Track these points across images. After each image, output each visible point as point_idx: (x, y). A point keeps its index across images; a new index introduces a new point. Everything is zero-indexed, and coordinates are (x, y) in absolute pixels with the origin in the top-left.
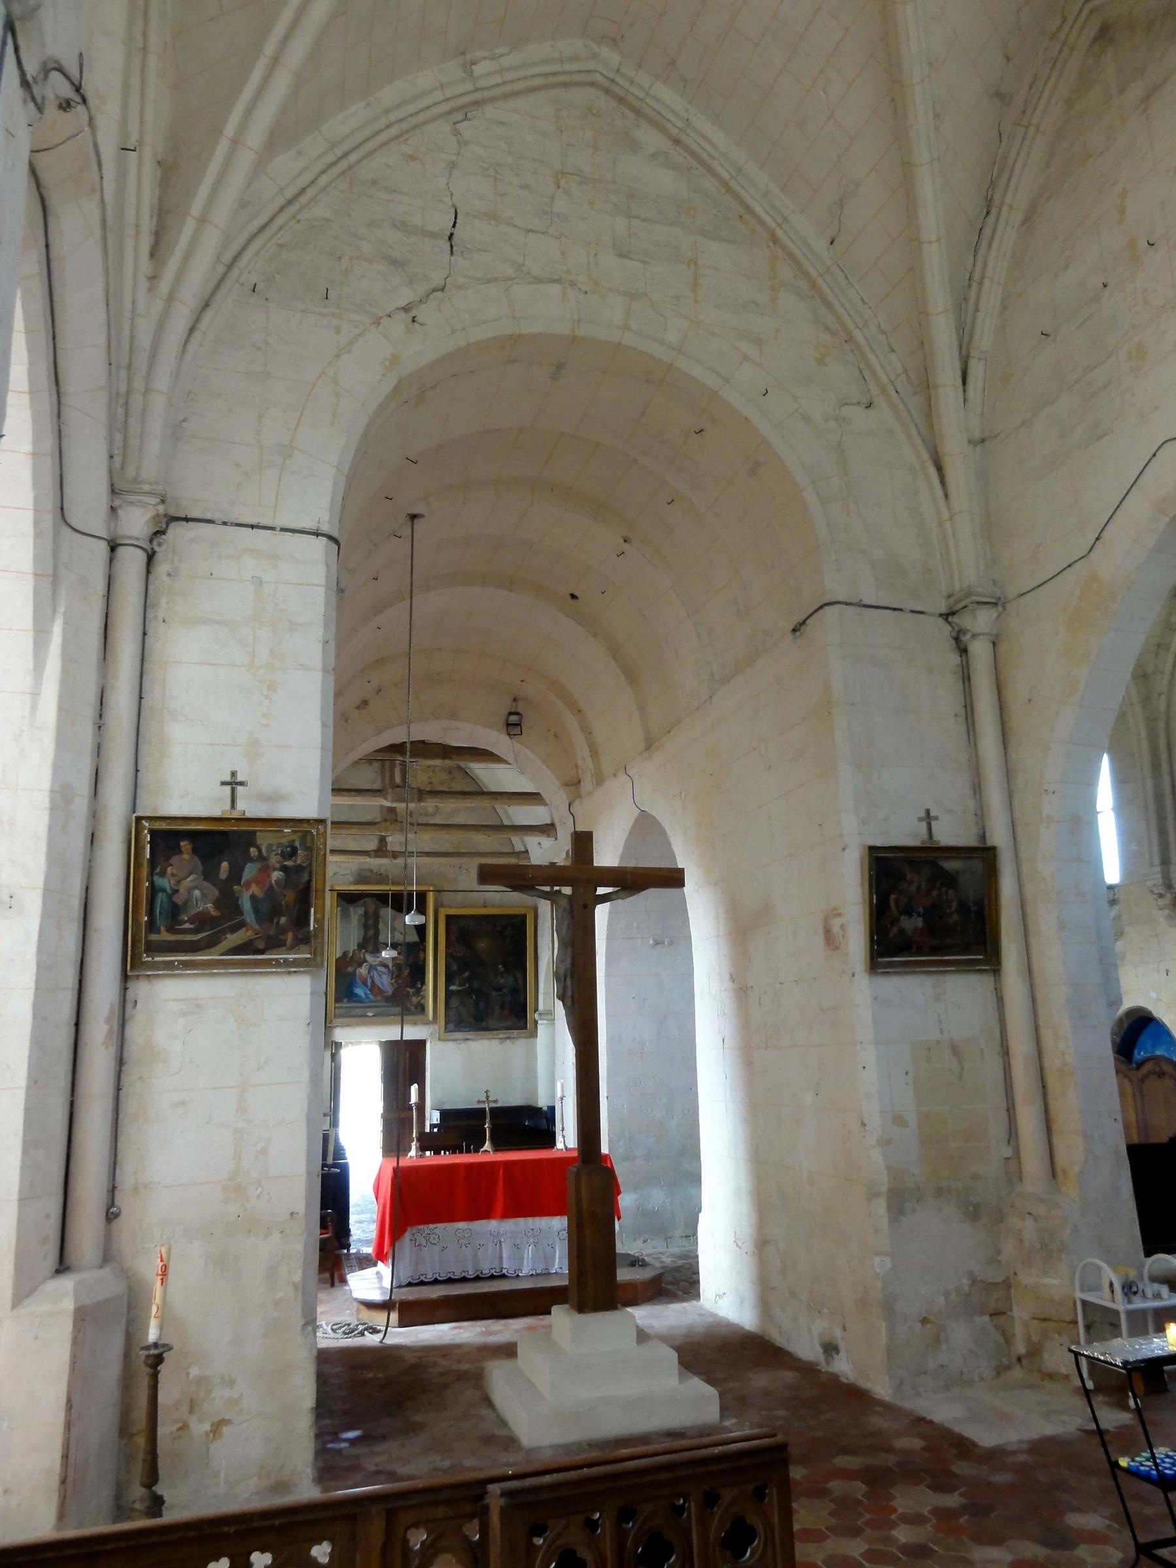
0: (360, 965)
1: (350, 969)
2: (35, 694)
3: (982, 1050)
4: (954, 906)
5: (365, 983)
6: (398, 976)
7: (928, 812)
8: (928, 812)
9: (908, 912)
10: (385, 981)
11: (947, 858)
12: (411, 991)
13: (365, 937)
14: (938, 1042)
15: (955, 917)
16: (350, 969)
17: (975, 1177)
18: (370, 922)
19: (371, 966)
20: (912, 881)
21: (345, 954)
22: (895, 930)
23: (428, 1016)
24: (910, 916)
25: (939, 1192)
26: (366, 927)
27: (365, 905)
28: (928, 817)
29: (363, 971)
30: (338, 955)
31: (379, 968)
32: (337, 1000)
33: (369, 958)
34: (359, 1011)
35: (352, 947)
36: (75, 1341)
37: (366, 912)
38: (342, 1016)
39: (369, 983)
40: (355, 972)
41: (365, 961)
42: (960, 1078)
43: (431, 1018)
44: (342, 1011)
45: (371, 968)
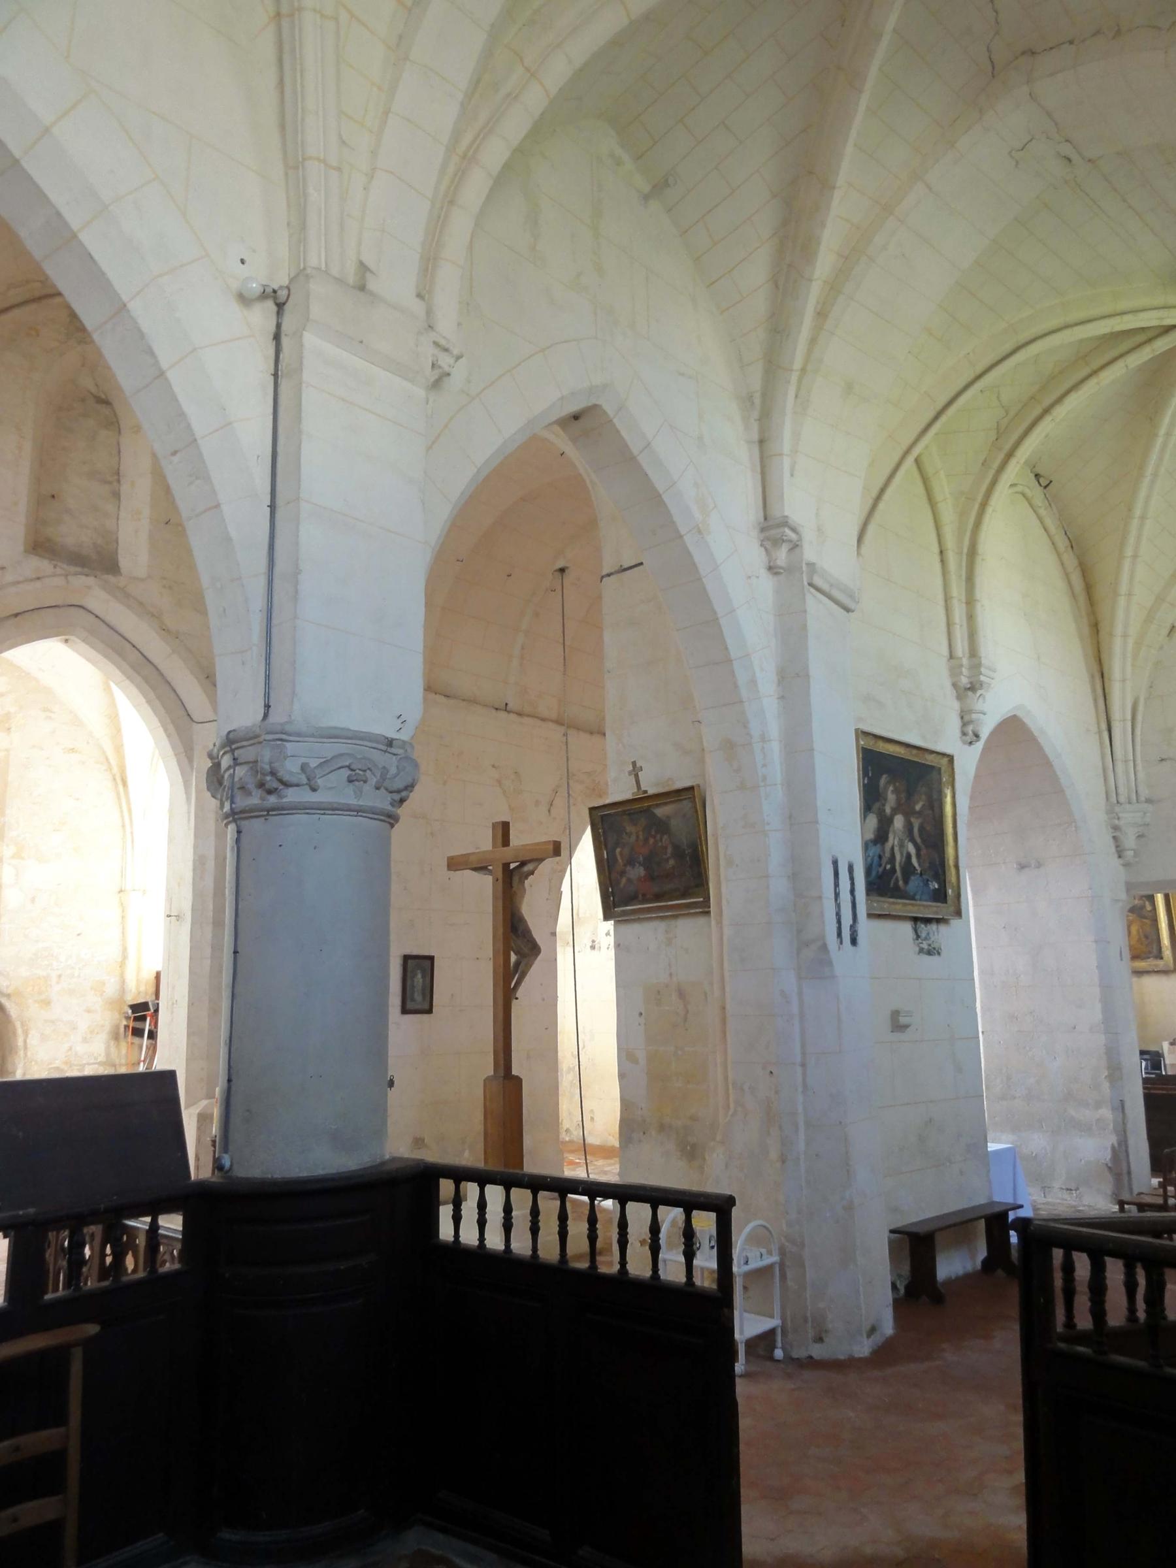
2: (189, 813)
3: (706, 994)
4: (669, 850)
7: (634, 764)
8: (634, 764)
9: (631, 862)
11: (657, 805)
14: (667, 986)
15: (672, 862)
17: (694, 1118)
20: (629, 835)
22: (624, 880)
24: (633, 866)
25: (662, 1128)
28: (636, 770)
36: (199, 1128)
42: (685, 1020)
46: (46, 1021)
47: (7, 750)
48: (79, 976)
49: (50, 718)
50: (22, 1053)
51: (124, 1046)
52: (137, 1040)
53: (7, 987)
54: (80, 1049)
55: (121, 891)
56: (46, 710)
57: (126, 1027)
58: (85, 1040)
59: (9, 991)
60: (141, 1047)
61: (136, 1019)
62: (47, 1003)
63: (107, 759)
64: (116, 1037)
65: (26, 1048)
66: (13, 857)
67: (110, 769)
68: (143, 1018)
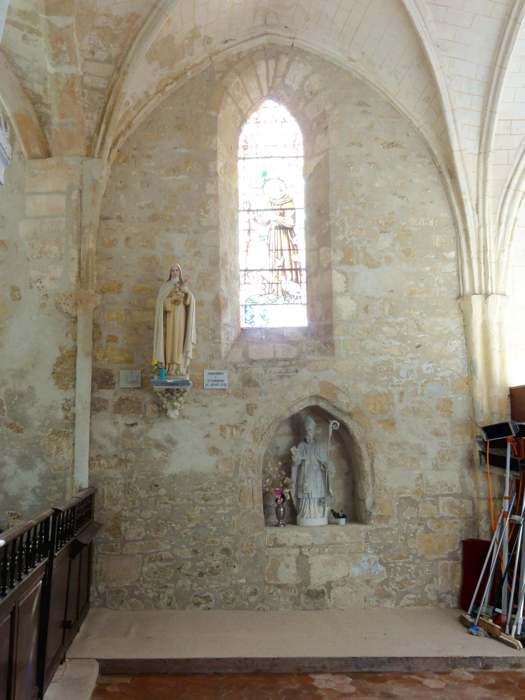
46: (391, 444)
47: (327, 151)
48: (422, 394)
49: (365, 112)
50: (369, 479)
51: (480, 474)
52: (497, 471)
53: (348, 405)
54: (432, 477)
55: (459, 297)
56: (360, 104)
57: (483, 453)
58: (436, 468)
59: (350, 409)
60: (502, 479)
61: (493, 445)
62: (390, 424)
63: (430, 150)
64: (471, 464)
65: (373, 474)
66: (341, 263)
67: (435, 162)
68: (503, 445)
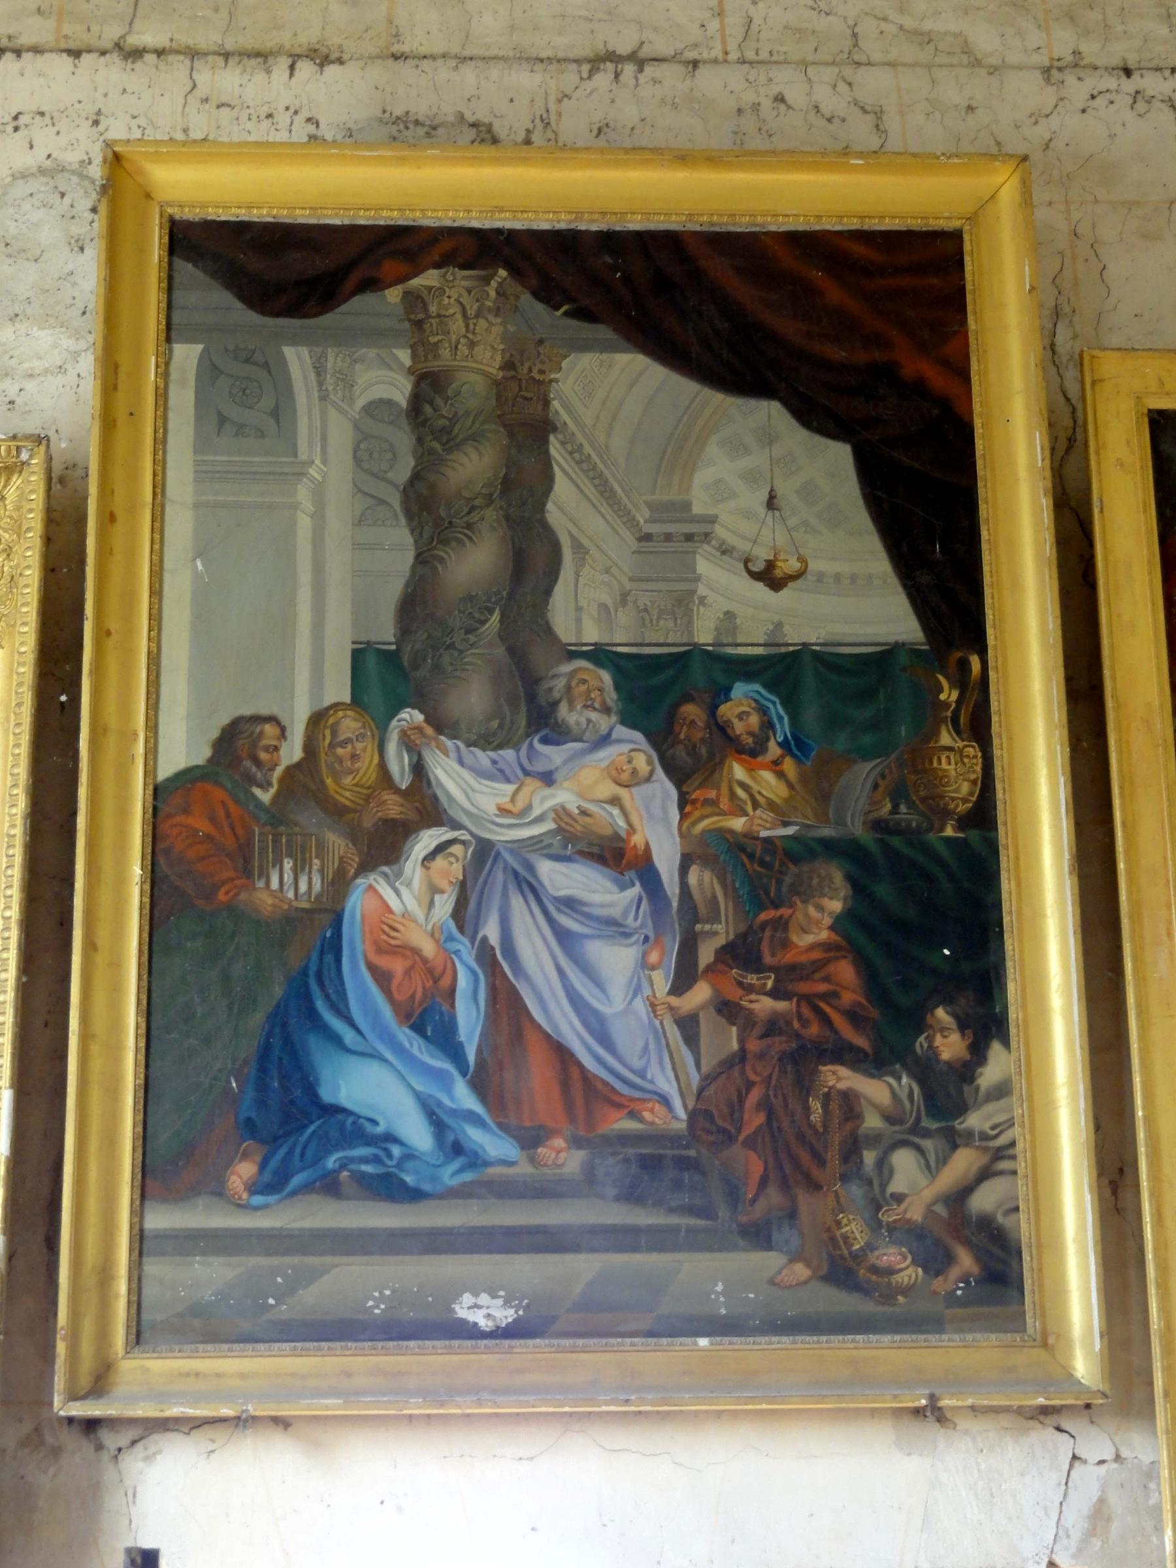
0: (383, 846)
1: (286, 885)
5: (429, 1019)
6: (741, 954)
10: (618, 998)
12: (877, 1092)
13: (415, 605)
16: (286, 885)
18: (473, 467)
19: (484, 852)
21: (237, 745)
23: (1050, 1342)
26: (429, 512)
27: (418, 317)
29: (408, 898)
30: (182, 749)
31: (564, 878)
32: (154, 1179)
33: (466, 784)
34: (371, 1283)
35: (309, 681)
37: (429, 384)
38: (205, 1327)
39: (469, 1018)
40: (329, 915)
41: (427, 808)
43: (1085, 1364)
44: (210, 1275)
45: (485, 869)
